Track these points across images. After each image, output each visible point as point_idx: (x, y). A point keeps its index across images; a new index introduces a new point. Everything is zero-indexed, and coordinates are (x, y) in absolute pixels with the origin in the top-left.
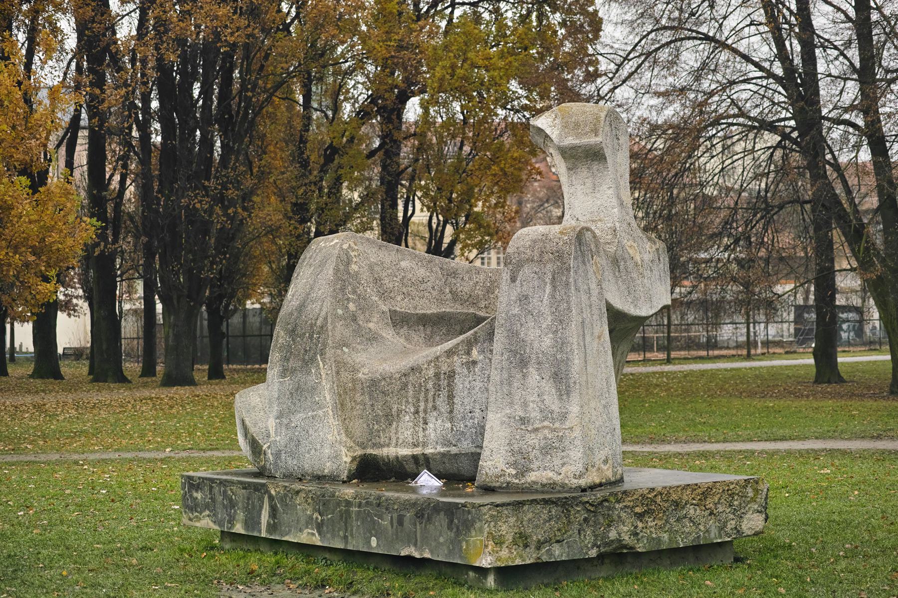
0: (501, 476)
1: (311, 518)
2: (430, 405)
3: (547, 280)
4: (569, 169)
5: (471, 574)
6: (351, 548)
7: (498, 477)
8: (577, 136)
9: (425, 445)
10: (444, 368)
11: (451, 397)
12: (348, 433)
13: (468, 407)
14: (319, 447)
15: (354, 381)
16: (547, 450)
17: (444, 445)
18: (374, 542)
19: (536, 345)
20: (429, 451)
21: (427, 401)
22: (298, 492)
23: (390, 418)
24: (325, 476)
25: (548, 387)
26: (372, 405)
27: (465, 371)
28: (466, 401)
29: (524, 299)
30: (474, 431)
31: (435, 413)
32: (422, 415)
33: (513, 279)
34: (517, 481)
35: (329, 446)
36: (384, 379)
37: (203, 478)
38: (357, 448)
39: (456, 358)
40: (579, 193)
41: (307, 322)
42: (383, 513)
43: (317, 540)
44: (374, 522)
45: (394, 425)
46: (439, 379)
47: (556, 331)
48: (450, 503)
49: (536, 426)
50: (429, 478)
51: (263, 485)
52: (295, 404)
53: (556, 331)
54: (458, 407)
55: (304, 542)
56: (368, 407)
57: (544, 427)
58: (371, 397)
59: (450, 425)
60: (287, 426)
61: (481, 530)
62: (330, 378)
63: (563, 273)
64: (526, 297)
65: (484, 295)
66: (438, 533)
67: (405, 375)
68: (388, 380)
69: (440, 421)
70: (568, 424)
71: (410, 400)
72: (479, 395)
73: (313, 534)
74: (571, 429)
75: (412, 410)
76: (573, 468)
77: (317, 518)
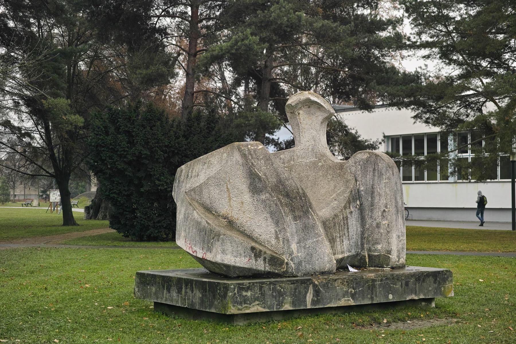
1: (347, 292)
5: (423, 303)
14: (322, 257)
18: (391, 297)
22: (336, 280)
43: (352, 303)
44: (390, 287)
51: (310, 279)
55: (343, 305)
60: (304, 247)
73: (349, 300)
77: (351, 291)
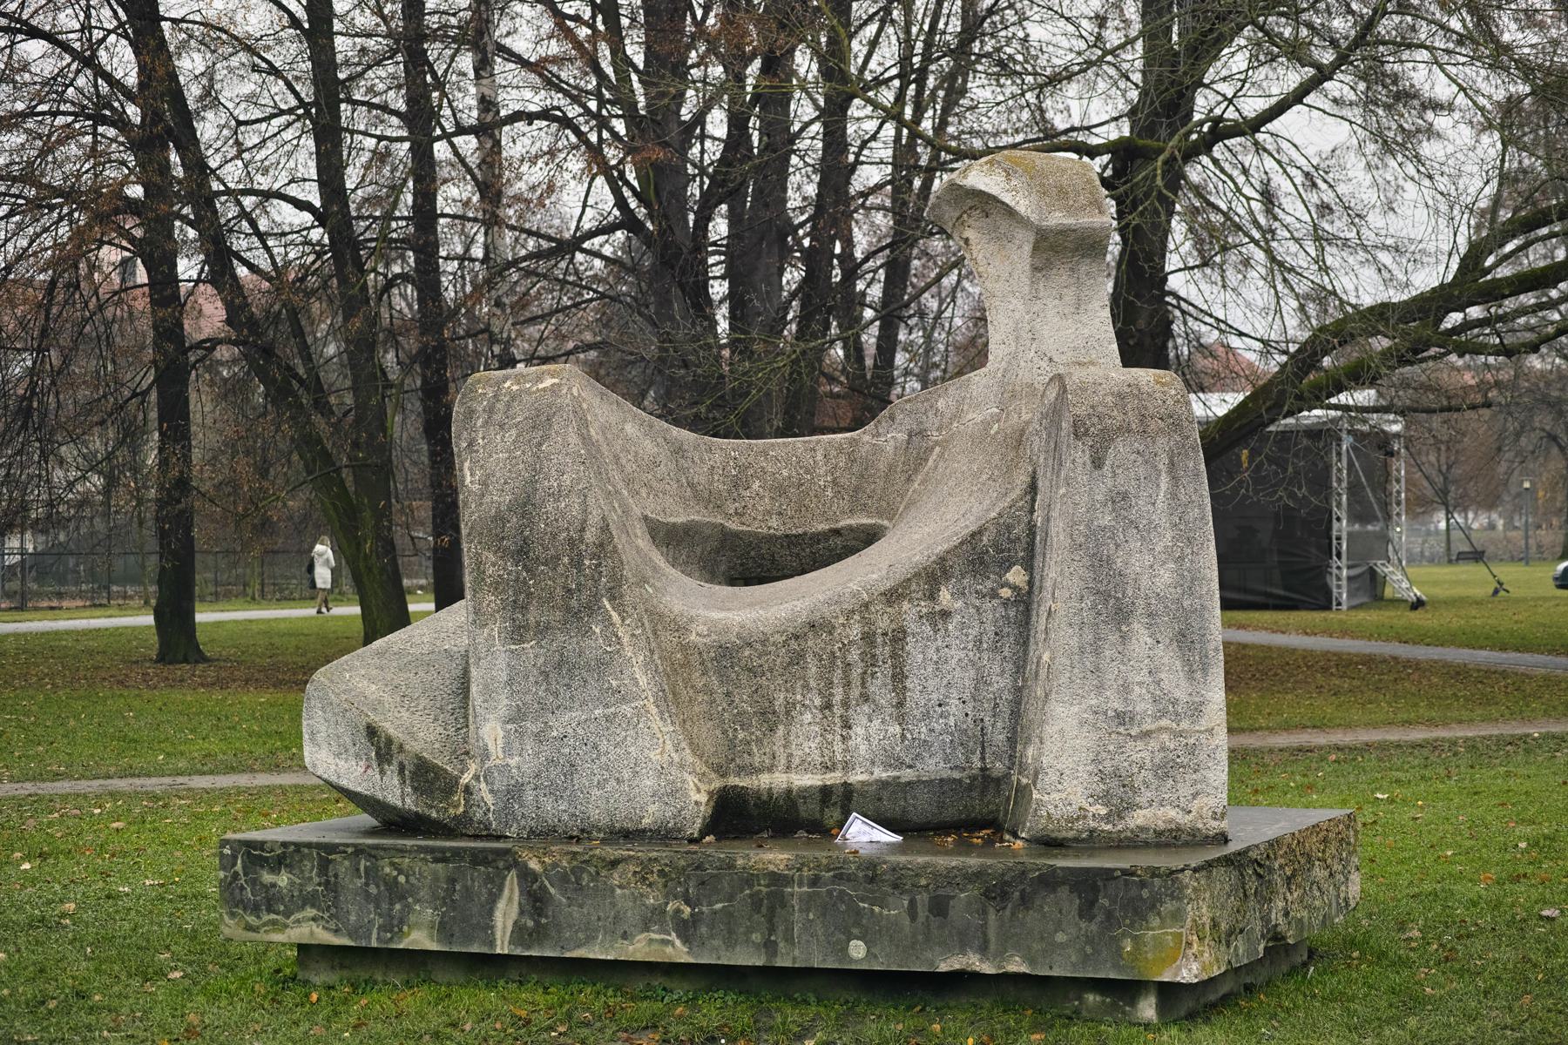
0: (1078, 819)
1: (660, 911)
2: (855, 692)
3: (1161, 466)
4: (1035, 269)
5: (1091, 998)
6: (788, 964)
7: (1072, 820)
8: (1069, 210)
9: (847, 766)
10: (883, 624)
11: (899, 677)
12: (696, 749)
13: (934, 696)
14: (626, 775)
15: (684, 648)
16: (1166, 770)
17: (887, 766)
18: (857, 949)
19: (1145, 582)
20: (857, 777)
21: (847, 684)
22: (614, 864)
23: (769, 718)
24: (644, 831)
25: (1167, 657)
26: (728, 694)
27: (928, 629)
28: (931, 684)
29: (1119, 499)
30: (948, 738)
31: (866, 708)
32: (838, 711)
33: (1097, 463)
34: (1109, 827)
35: (653, 768)
36: (750, 645)
37: (296, 844)
38: (713, 775)
39: (906, 605)
40: (1051, 313)
41: (554, 536)
42: (886, 894)
43: (679, 952)
44: (859, 913)
45: (781, 730)
46: (872, 644)
47: (1182, 558)
48: (1088, 870)
49: (1146, 727)
50: (867, 829)
51: (507, 852)
52: (556, 694)
53: (1182, 558)
54: (914, 696)
55: (639, 957)
56: (719, 697)
57: (1160, 729)
58: (723, 678)
59: (898, 729)
60: (539, 737)
61: (1178, 916)
62: (643, 644)
63: (1187, 455)
64: (1125, 496)
65: (729, 492)
66: (1051, 927)
67: (797, 637)
68: (758, 646)
69: (876, 722)
70: (1204, 724)
71: (813, 683)
72: (957, 673)
73: (665, 942)
74: (1210, 731)
75: (818, 702)
76: (1212, 802)
77: (678, 911)
